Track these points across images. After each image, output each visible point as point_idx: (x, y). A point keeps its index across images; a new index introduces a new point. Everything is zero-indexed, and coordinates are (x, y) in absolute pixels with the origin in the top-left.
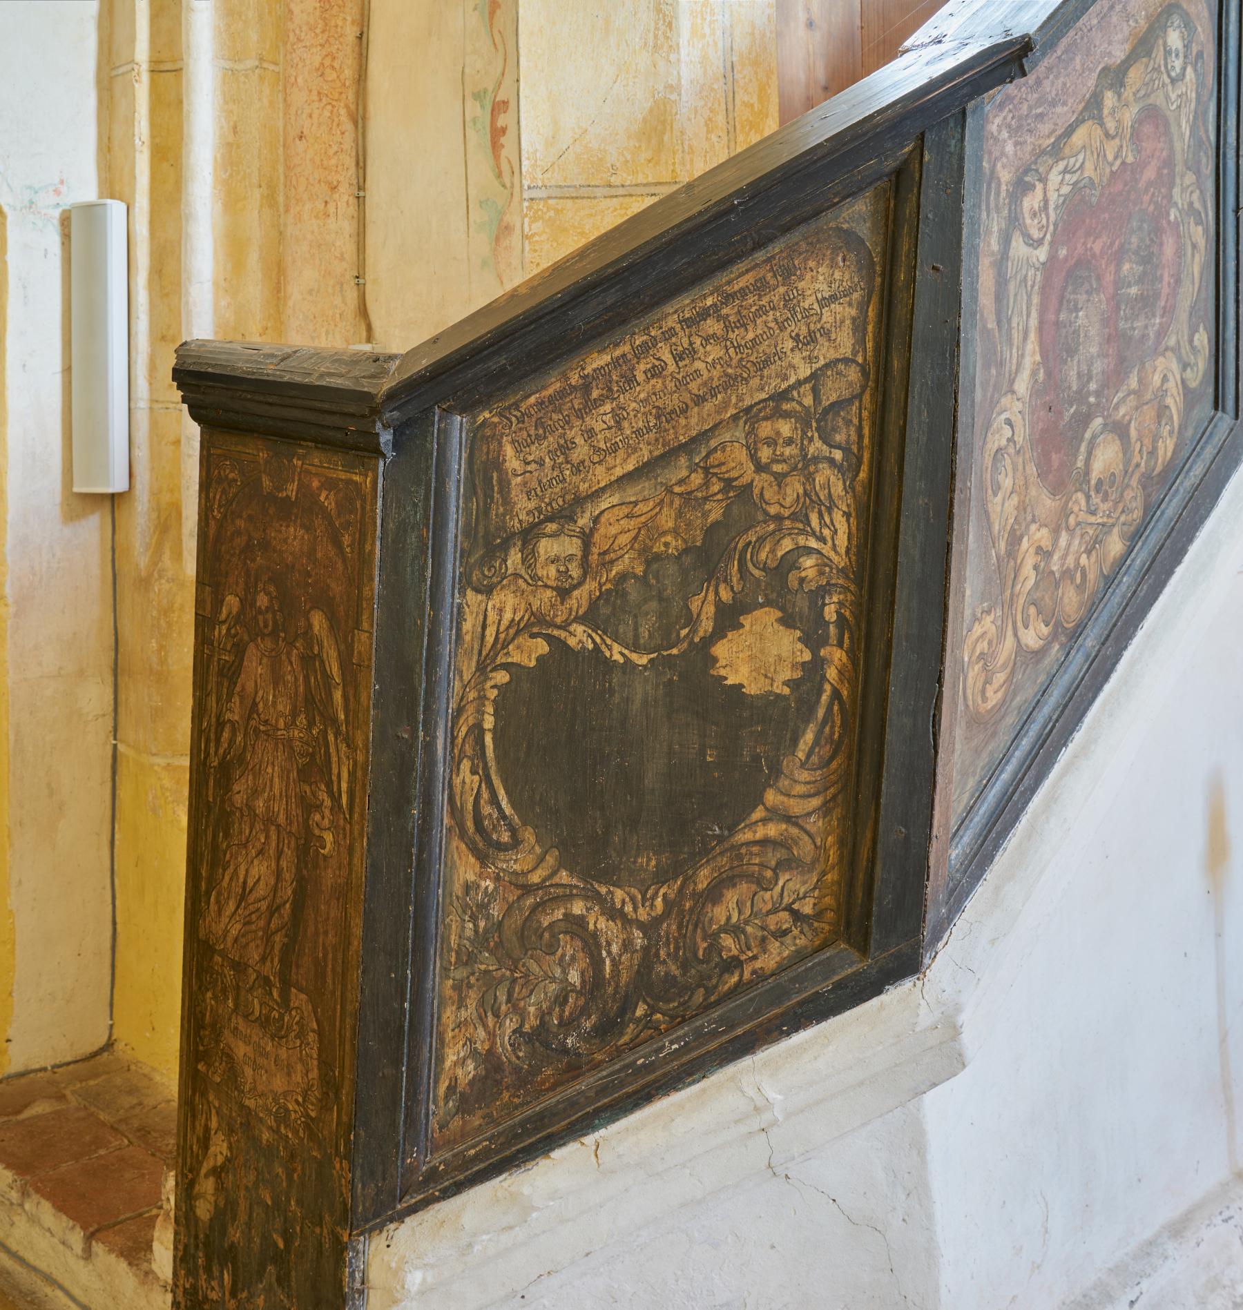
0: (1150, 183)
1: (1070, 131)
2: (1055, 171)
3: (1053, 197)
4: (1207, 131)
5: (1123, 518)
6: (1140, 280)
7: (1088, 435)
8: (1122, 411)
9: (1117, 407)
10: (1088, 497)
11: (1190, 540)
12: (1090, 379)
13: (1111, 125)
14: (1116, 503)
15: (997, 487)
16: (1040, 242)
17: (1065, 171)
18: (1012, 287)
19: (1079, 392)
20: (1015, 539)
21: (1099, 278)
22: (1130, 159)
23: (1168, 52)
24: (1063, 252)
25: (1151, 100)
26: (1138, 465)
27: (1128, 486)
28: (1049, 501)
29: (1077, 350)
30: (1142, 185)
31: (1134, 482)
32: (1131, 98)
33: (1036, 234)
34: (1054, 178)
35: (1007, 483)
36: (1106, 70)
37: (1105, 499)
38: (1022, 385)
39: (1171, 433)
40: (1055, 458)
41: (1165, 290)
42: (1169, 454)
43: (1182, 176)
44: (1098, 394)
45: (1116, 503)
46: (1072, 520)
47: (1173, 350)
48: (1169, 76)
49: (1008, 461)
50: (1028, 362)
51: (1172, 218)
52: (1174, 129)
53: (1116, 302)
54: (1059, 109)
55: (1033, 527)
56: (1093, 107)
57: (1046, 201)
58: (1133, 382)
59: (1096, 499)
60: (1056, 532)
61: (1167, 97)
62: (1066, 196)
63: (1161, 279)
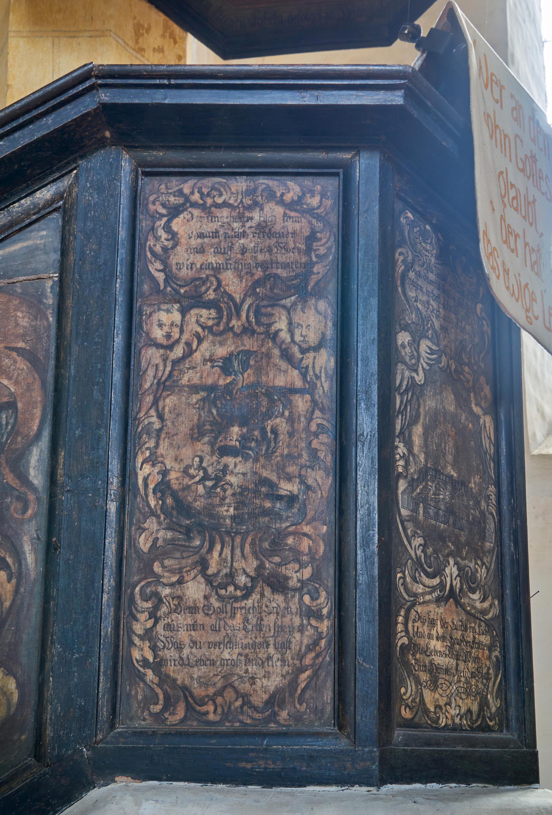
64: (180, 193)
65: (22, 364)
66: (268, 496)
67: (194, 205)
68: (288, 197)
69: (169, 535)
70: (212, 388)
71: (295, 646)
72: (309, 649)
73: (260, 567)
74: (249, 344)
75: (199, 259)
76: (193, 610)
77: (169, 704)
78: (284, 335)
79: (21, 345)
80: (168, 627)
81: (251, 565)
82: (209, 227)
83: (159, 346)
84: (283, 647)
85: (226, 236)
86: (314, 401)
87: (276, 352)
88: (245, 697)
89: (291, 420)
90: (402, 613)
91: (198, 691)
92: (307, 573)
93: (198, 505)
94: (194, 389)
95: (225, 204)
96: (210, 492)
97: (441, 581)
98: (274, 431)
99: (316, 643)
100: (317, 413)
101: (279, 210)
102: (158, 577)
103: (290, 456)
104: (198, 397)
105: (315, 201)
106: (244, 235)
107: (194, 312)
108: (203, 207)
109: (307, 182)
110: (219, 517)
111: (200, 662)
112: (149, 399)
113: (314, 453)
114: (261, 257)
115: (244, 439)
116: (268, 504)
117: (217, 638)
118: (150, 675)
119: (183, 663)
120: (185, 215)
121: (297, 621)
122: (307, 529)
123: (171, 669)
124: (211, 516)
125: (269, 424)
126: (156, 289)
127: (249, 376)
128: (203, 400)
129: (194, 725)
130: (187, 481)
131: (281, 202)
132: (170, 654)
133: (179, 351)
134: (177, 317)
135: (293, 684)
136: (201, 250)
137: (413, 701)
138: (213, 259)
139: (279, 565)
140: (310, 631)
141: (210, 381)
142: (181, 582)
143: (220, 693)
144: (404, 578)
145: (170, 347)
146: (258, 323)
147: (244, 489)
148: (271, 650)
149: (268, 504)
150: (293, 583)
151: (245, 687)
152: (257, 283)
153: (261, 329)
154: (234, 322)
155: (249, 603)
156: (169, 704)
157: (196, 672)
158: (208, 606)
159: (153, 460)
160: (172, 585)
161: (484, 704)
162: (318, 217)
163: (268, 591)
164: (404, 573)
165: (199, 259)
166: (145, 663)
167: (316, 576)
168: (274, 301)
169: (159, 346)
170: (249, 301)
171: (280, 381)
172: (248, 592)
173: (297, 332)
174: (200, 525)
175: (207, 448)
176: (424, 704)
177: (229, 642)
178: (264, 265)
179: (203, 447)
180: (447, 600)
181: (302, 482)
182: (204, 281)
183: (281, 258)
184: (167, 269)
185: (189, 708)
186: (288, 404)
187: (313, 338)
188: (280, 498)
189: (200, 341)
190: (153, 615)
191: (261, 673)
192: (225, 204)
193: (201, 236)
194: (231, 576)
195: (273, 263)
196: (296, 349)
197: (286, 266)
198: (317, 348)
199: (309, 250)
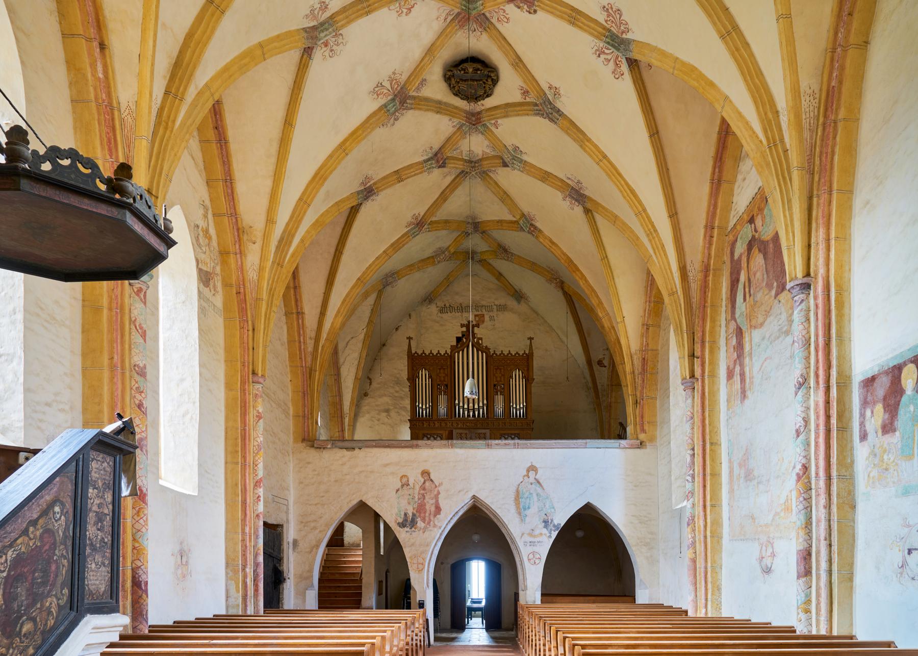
1: (16, 540)
2: (11, 551)
3: (9, 558)
4: (69, 533)
6: (42, 578)
7: (21, 622)
8: (34, 614)
10: (20, 639)
11: (59, 648)
12: (22, 606)
13: (32, 536)
14: (31, 640)
16: (4, 571)
17: (14, 551)
19: (17, 610)
21: (26, 579)
22: (39, 544)
23: (54, 513)
24: (13, 573)
25: (48, 527)
26: (40, 628)
27: (36, 634)
30: (43, 551)
31: (38, 633)
34: (10, 553)
36: (30, 521)
37: (27, 639)
39: (53, 619)
40: (8, 629)
41: (52, 579)
42: (52, 624)
43: (59, 547)
44: (24, 610)
45: (31, 640)
46: (14, 645)
47: (54, 595)
48: (55, 519)
51: (55, 559)
52: (56, 534)
53: (32, 584)
54: (12, 534)
56: (25, 532)
57: (6, 560)
58: (39, 606)
59: (23, 639)
60: (8, 650)
61: (54, 526)
62: (14, 558)
63: (50, 576)
65: (70, 500)
70: (96, 512)
77: (89, 596)
80: (90, 576)
84: (104, 580)
91: (94, 592)
103: (106, 532)
115: (101, 526)
127: (101, 510)
132: (90, 582)
157: (94, 587)
185: (92, 596)
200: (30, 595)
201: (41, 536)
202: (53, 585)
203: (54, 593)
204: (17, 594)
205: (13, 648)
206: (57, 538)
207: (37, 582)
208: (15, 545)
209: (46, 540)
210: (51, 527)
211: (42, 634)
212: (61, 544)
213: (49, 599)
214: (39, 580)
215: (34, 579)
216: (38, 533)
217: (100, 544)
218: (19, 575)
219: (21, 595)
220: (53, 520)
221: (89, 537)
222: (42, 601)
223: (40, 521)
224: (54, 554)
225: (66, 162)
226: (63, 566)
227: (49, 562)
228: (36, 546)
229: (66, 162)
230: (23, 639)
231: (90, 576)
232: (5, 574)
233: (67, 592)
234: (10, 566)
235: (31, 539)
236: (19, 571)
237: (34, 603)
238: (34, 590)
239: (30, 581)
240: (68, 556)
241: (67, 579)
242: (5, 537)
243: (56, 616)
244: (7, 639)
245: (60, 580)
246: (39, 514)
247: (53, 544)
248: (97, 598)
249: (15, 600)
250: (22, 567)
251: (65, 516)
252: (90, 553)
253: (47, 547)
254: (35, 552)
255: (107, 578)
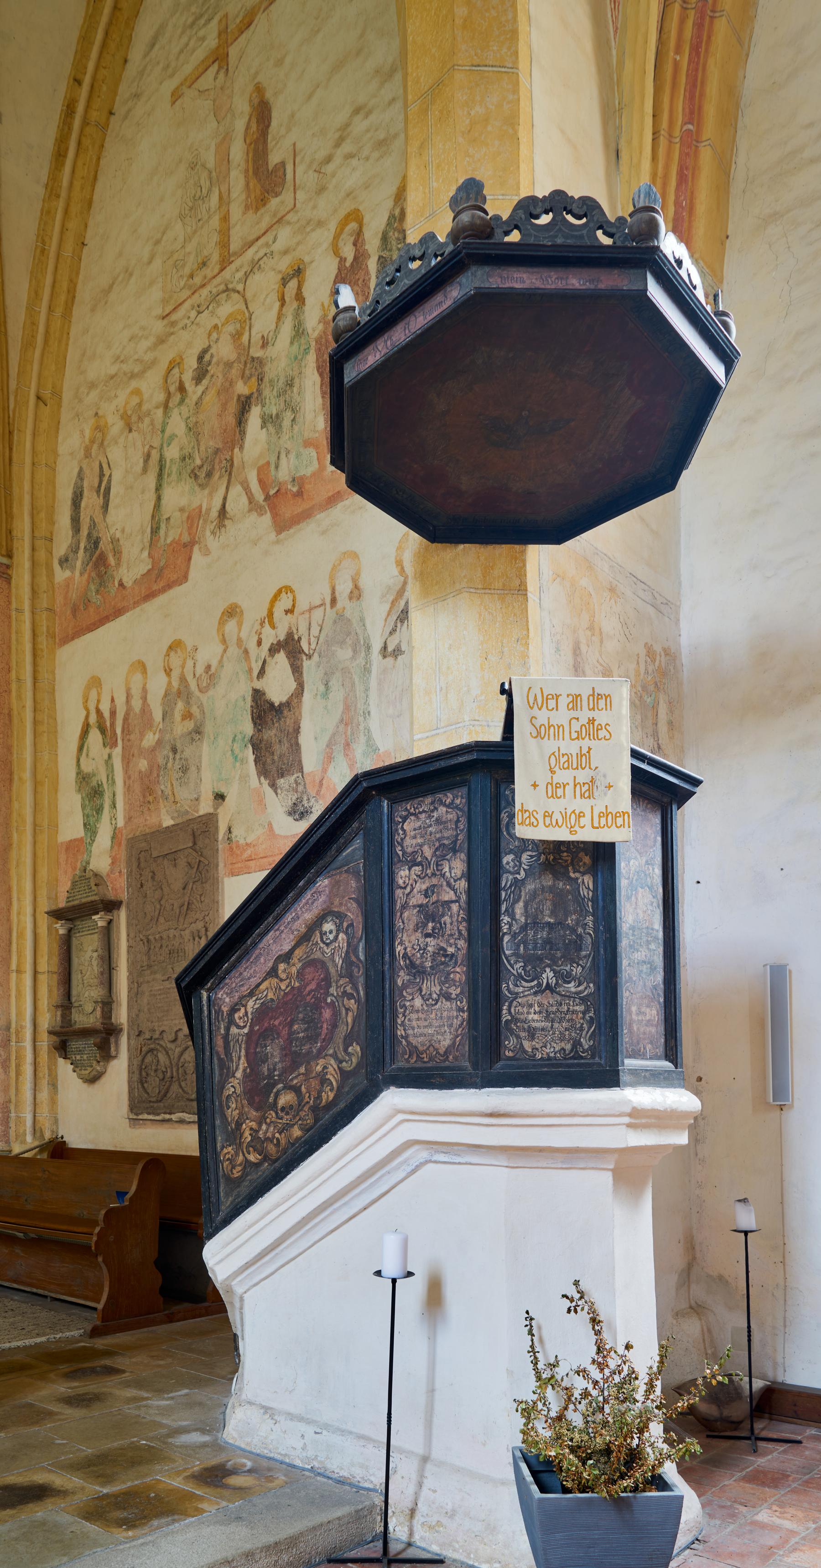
0: (312, 991)
2: (251, 1001)
3: (250, 1010)
4: (358, 957)
5: (300, 1122)
6: (306, 1030)
7: (275, 1090)
8: (295, 1082)
9: (292, 1080)
10: (277, 1113)
12: (275, 1070)
13: (283, 976)
14: (294, 1117)
15: (229, 1107)
16: (245, 1027)
17: (257, 999)
18: (232, 1044)
19: (269, 1075)
20: (239, 1124)
21: (278, 1034)
22: (297, 984)
23: (322, 934)
24: (257, 1028)
25: (312, 957)
26: (308, 1102)
27: (301, 1110)
28: (254, 1113)
29: (267, 1060)
31: (306, 1109)
32: (297, 961)
33: (242, 1024)
34: (251, 1003)
35: (234, 1106)
36: (280, 956)
37: (287, 1114)
38: (239, 1074)
39: (331, 1090)
40: (257, 1099)
41: (325, 1031)
42: (331, 1098)
44: (279, 1076)
45: (294, 1117)
46: (268, 1120)
47: (331, 1055)
48: (324, 943)
49: (233, 1099)
50: (241, 1067)
51: (329, 1000)
52: (330, 965)
53: (290, 1040)
54: (252, 980)
55: (247, 1121)
57: (246, 1013)
58: (302, 1070)
59: (281, 1114)
61: (323, 953)
63: (322, 1027)
64: (406, 810)
65: (355, 905)
66: (443, 955)
67: (412, 814)
68: (447, 802)
69: (408, 977)
70: (420, 906)
71: (454, 1026)
72: (460, 1026)
73: (441, 989)
74: (434, 881)
75: (414, 842)
76: (418, 1011)
77: (410, 1055)
78: (448, 874)
79: (353, 896)
81: (437, 989)
82: (418, 824)
83: (401, 888)
84: (451, 1026)
85: (424, 828)
86: (460, 906)
87: (445, 883)
88: (436, 1050)
89: (451, 917)
90: (507, 1004)
91: (421, 1048)
92: (459, 990)
93: (418, 962)
94: (414, 907)
95: (424, 811)
96: (422, 956)
97: (539, 982)
98: (445, 924)
99: (462, 1024)
100: (461, 912)
101: (444, 809)
102: (405, 997)
103: (451, 935)
104: (415, 911)
105: (458, 801)
106: (431, 825)
107: (413, 868)
108: (415, 815)
109: (455, 792)
110: (426, 968)
111: (421, 1035)
112: (399, 914)
113: (460, 932)
114: (438, 836)
115: (434, 928)
116: (443, 959)
117: (426, 1023)
118: (404, 1042)
119: (415, 1036)
120: (409, 820)
121: (455, 1014)
122: (458, 969)
123: (411, 1039)
124: (422, 967)
125: (443, 920)
126: (400, 861)
127: (434, 898)
128: (419, 911)
129: (419, 1065)
130: (414, 952)
131: (445, 805)
132: (410, 1032)
133: (408, 889)
134: (407, 872)
135: (454, 1043)
136: (415, 837)
137: (515, 1047)
138: (420, 841)
139: (448, 988)
140: (460, 1018)
141: (420, 902)
142: (413, 999)
143: (428, 1048)
144: (508, 986)
145: (405, 888)
146: (438, 870)
147: (434, 953)
148: (446, 1028)
149: (443, 959)
150: (453, 996)
151: (437, 1046)
152: (437, 849)
153: (438, 873)
154: (429, 871)
155: (437, 1006)
156: (410, 1055)
157: (420, 1039)
158: (423, 1009)
159: (401, 943)
160: (410, 1001)
161: (576, 1044)
162: (460, 810)
163: (444, 1000)
164: (508, 984)
165: (414, 842)
166: (402, 1037)
167: (462, 993)
168: (443, 858)
169: (401, 888)
170: (434, 859)
171: (446, 898)
172: (437, 1001)
173: (453, 872)
174: (419, 972)
175: (420, 935)
176: (523, 1048)
177: (430, 1026)
178: (439, 840)
179: (418, 934)
180: (543, 992)
181: (456, 947)
182: (417, 852)
183: (446, 835)
184: (403, 850)
185: (418, 1056)
186: (450, 909)
187: (459, 874)
188: (448, 955)
189: (416, 882)
190: (404, 1015)
191: (442, 1039)
192: (424, 811)
193: (415, 829)
194: (430, 994)
195: (443, 838)
196: (452, 881)
197: (448, 838)
198: (460, 879)
199: (457, 827)
200: (286, 1055)
201: (300, 974)
202: (329, 1040)
203: (331, 1052)
204: (267, 1054)
205: (266, 1123)
206: (332, 971)
207: (298, 1038)
208: (257, 992)
209: (309, 977)
210: (318, 955)
211: (313, 1111)
212: (341, 976)
213: (321, 1062)
214: (301, 1035)
215: (291, 1033)
216: (294, 970)
217: (433, 960)
218: (266, 1030)
219: (272, 1055)
220: (322, 945)
221: (405, 954)
222: (308, 1063)
223: (297, 952)
224: (327, 994)
225: (545, 219)
226: (347, 1010)
227: (317, 1007)
228: (293, 988)
229: (545, 219)
230: (281, 1114)
231: (409, 1020)
232: (246, 1030)
233: (358, 1049)
234: (252, 1019)
235: (281, 980)
236: (266, 1025)
237: (294, 1066)
238: (293, 1049)
239: (286, 1037)
240: (358, 993)
241: (356, 1029)
242: (242, 985)
243: (338, 1088)
244: (257, 1110)
245: (342, 1031)
246: (293, 944)
247: (323, 980)
248: (431, 1059)
249: (264, 1062)
250: (271, 1019)
251: (346, 933)
252: (409, 981)
253: (313, 986)
254: (290, 997)
255: (456, 1022)
